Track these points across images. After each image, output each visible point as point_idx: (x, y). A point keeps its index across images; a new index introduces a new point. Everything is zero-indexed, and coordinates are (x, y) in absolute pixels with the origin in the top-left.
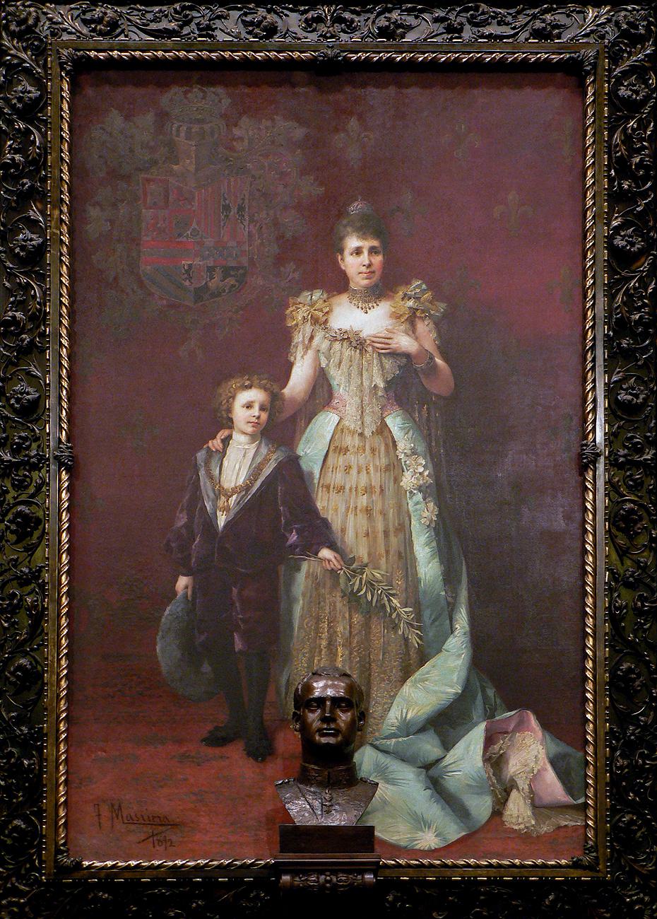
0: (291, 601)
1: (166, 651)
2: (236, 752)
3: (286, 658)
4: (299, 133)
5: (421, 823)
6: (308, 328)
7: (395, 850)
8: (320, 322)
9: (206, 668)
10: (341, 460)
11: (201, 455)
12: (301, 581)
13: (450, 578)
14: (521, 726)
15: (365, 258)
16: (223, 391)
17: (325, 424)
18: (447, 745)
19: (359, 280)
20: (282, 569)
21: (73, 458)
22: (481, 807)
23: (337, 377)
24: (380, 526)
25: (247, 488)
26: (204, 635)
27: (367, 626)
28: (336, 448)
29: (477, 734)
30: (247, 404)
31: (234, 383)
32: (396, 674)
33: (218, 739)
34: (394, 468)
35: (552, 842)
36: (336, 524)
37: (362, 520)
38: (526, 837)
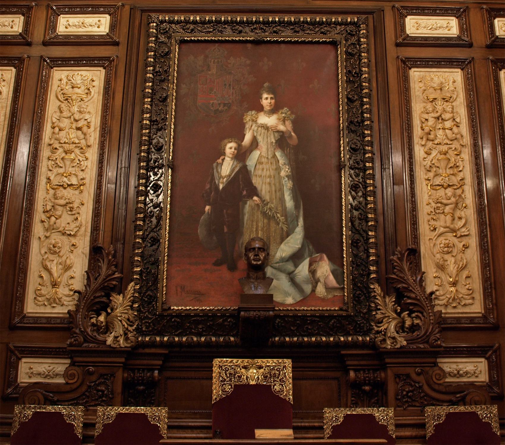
0: (243, 214)
1: (201, 232)
2: (224, 268)
3: (241, 234)
4: (248, 62)
5: (287, 294)
6: (250, 123)
8: (255, 121)
9: (215, 238)
10: (261, 167)
11: (215, 165)
13: (297, 207)
14: (321, 259)
15: (269, 101)
16: (223, 143)
17: (256, 154)
18: (296, 266)
19: (267, 108)
20: (241, 203)
21: (173, 165)
22: (308, 289)
23: (260, 139)
24: (273, 189)
25: (230, 176)
27: (269, 224)
28: (259, 162)
29: (306, 262)
30: (230, 147)
31: (226, 141)
32: (278, 240)
33: (217, 264)
34: (278, 169)
36: (259, 188)
37: (268, 187)
38: (323, 300)
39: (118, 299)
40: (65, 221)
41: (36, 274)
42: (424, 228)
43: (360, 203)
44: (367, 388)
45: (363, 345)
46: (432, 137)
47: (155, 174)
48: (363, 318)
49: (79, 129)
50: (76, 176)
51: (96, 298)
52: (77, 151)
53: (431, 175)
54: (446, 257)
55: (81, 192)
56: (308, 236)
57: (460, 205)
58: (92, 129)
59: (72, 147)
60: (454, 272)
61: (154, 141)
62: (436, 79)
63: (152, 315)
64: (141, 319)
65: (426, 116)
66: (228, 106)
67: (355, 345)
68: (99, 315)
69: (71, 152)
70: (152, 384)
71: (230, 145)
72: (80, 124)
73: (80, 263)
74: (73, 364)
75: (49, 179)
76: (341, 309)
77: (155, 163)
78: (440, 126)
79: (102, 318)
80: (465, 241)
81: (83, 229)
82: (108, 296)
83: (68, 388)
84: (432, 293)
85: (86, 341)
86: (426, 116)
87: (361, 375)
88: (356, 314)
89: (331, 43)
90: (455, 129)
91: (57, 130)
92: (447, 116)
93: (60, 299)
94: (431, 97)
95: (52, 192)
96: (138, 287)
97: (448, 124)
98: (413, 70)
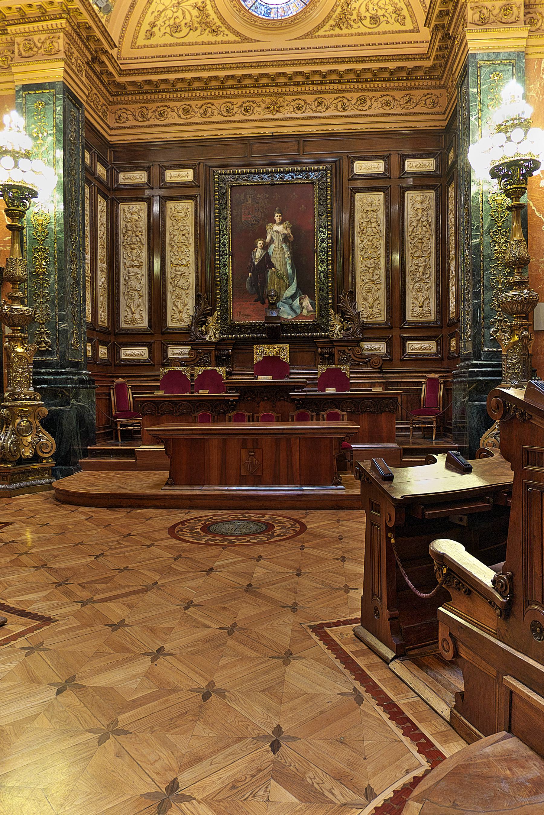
0: (268, 277)
1: (247, 286)
5: (289, 314)
7: (284, 319)
12: (269, 274)
13: (293, 272)
14: (305, 297)
17: (273, 246)
18: (293, 301)
19: (278, 221)
22: (299, 311)
26: (254, 282)
27: (280, 281)
28: (274, 250)
30: (260, 243)
32: (285, 289)
35: (310, 317)
38: (306, 316)
39: (210, 319)
40: (182, 282)
41: (171, 308)
42: (358, 280)
43: (325, 269)
44: (327, 356)
45: (325, 337)
46: (364, 232)
47: (224, 258)
48: (325, 324)
49: (184, 235)
50: (185, 260)
51: (200, 319)
52: (184, 247)
53: (364, 252)
54: (368, 294)
55: (188, 267)
56: (298, 286)
57: (377, 268)
58: (190, 234)
59: (181, 245)
60: (372, 301)
61: (222, 241)
62: (369, 199)
63: (227, 326)
64: (222, 328)
65: (362, 221)
66: (258, 221)
67: (321, 337)
68: (202, 327)
69: (181, 247)
70: (228, 356)
71: (259, 242)
72: (184, 232)
73: (191, 303)
74: (192, 349)
75: (171, 261)
76: (314, 321)
77: (223, 252)
78: (370, 226)
79: (203, 328)
80: (378, 286)
81: (191, 285)
82: (206, 318)
83: (190, 360)
84: (359, 312)
85: (197, 339)
86: (362, 221)
87: (324, 350)
88: (321, 324)
89: (312, 183)
90: (377, 228)
91: (172, 236)
92: (373, 220)
93: (183, 319)
94: (366, 210)
95: (174, 268)
96: (219, 313)
97: (374, 225)
98: (357, 194)
